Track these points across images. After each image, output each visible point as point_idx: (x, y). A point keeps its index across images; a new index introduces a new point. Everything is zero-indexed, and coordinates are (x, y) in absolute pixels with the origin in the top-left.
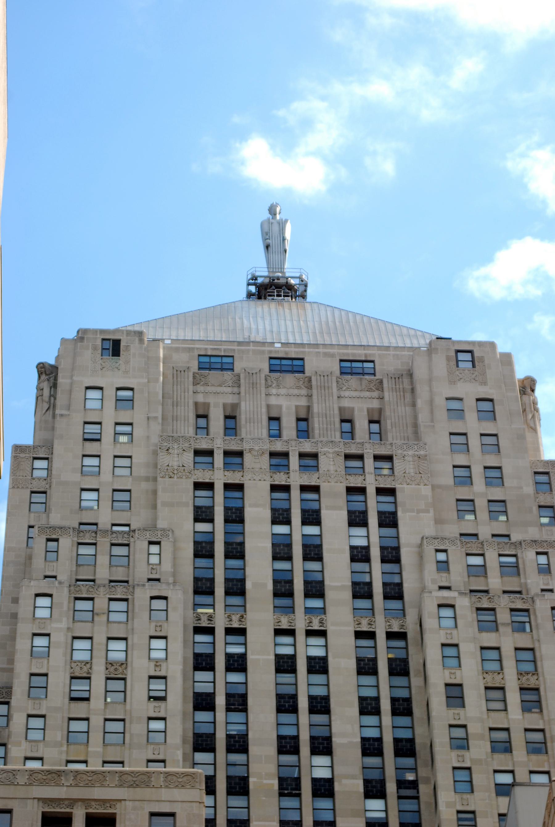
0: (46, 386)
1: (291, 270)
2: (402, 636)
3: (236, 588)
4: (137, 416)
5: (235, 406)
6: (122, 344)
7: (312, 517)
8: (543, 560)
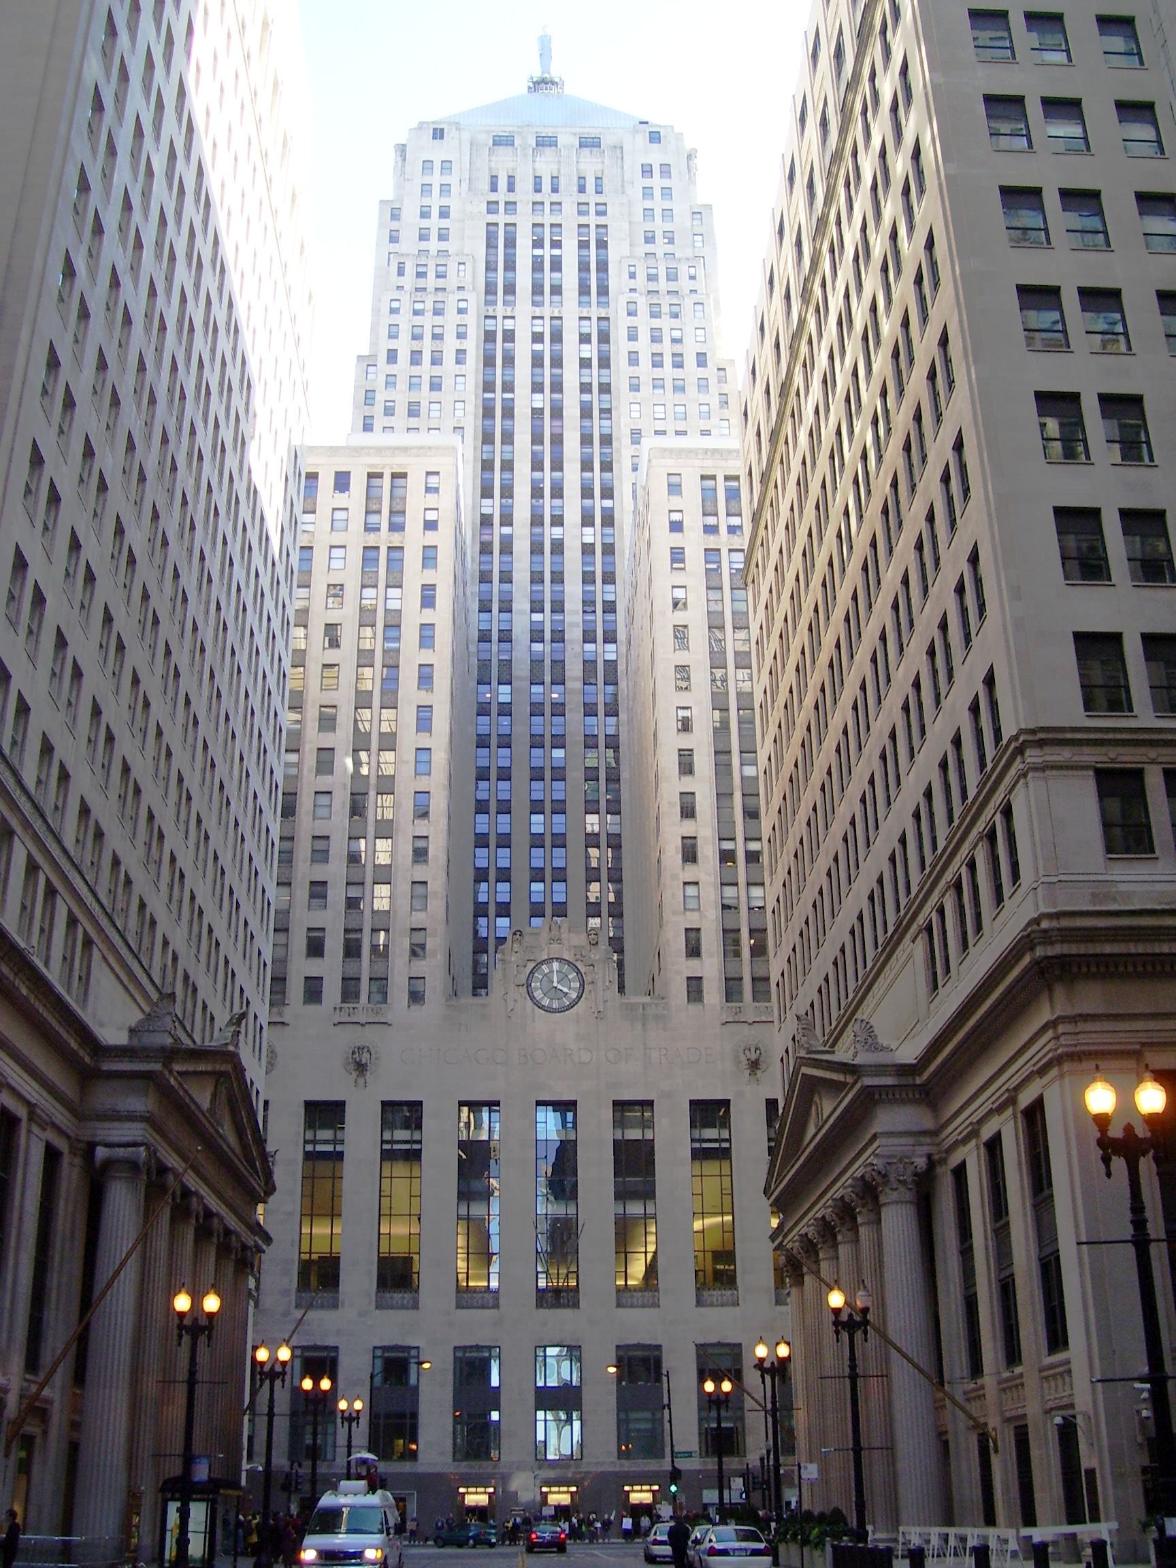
1: (555, 74)
3: (510, 289)
4: (452, 179)
5: (513, 170)
7: (556, 244)
8: (692, 271)
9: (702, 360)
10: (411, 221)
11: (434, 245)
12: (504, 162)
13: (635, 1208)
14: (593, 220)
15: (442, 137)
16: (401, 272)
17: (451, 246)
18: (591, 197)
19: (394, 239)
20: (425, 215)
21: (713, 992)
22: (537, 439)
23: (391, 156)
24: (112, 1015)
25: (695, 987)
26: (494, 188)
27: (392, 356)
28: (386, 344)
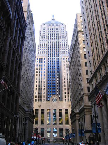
3: (50, 39)
9: (66, 45)
10: (42, 32)
11: (44, 35)
12: (50, 27)
13: (61, 117)
14: (57, 32)
17: (45, 35)
18: (57, 30)
19: (41, 34)
20: (43, 32)
21: (67, 101)
22: (53, 52)
23: (40, 26)
24: (27, 109)
25: (65, 100)
26: (49, 30)
27: (41, 45)
28: (40, 44)
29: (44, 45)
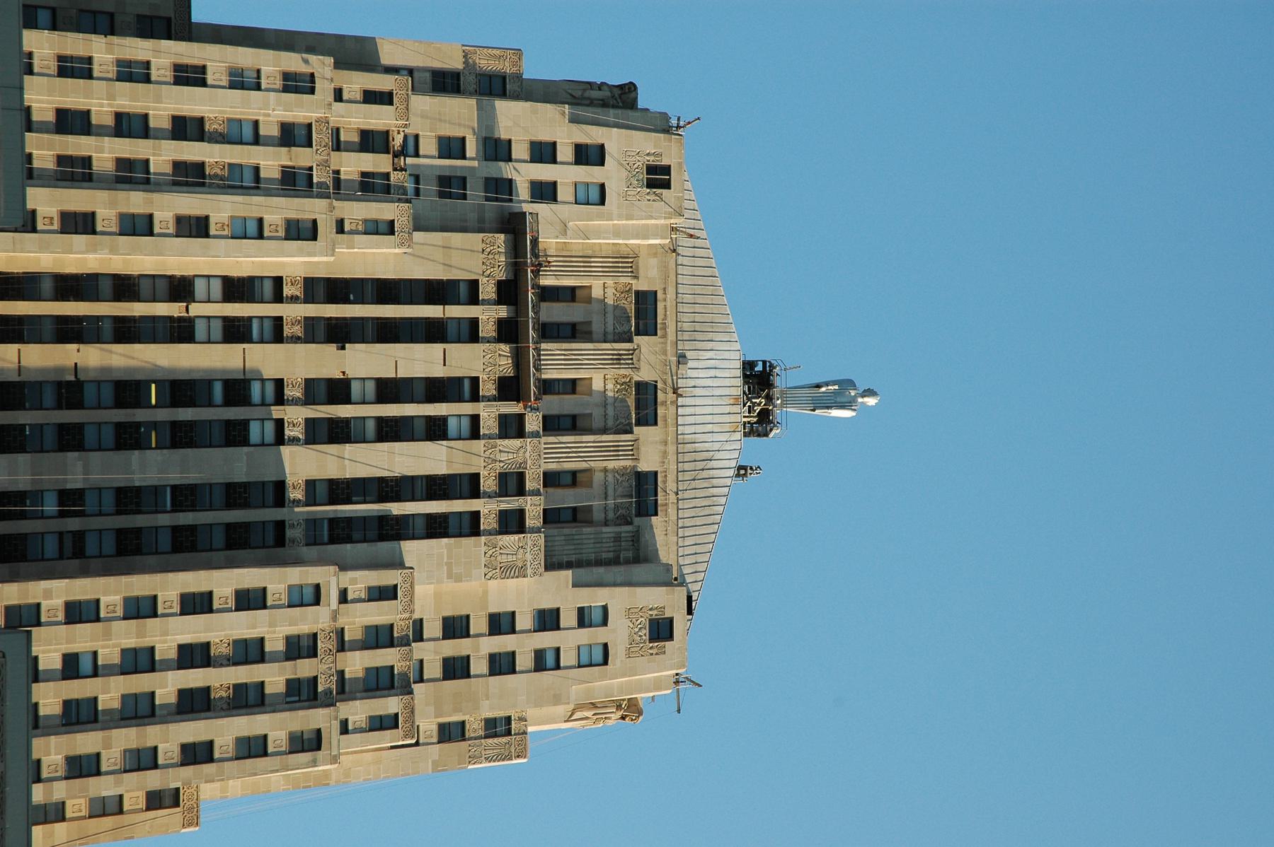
0: (605, 93)
2: (280, 541)
3: (340, 333)
6: (664, 191)
15: (651, 184)
16: (372, 97)
29: (190, 176)
